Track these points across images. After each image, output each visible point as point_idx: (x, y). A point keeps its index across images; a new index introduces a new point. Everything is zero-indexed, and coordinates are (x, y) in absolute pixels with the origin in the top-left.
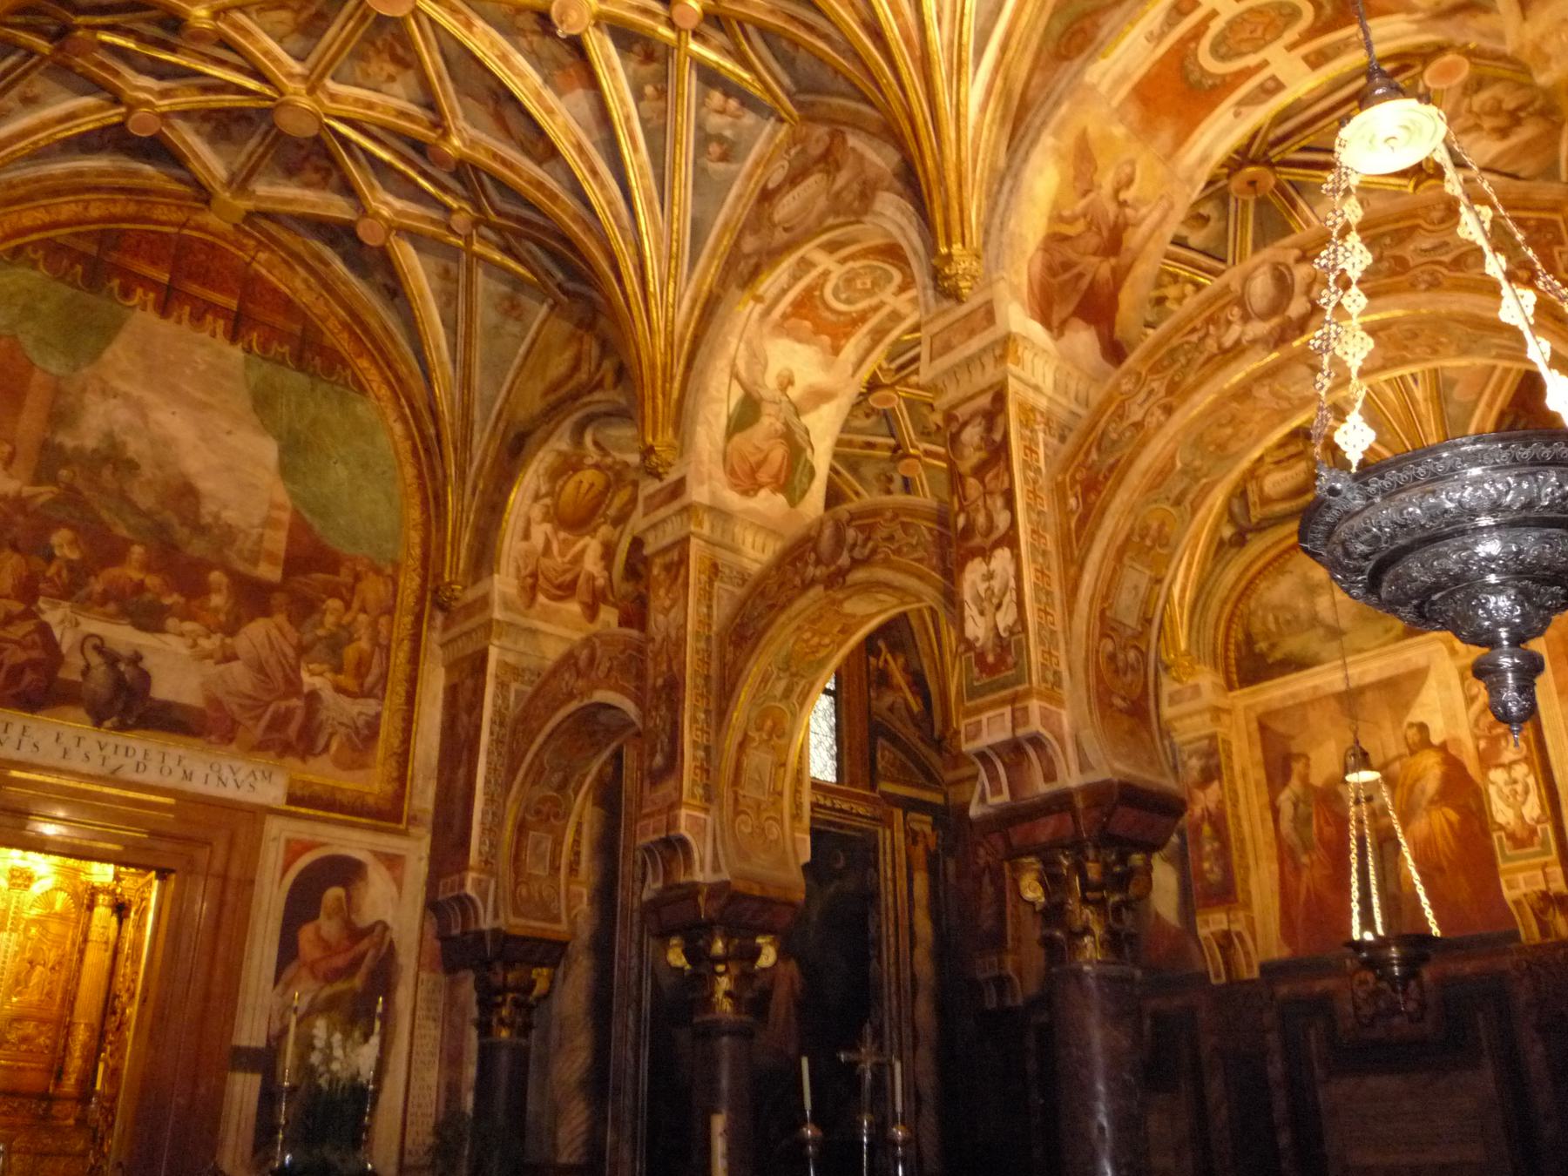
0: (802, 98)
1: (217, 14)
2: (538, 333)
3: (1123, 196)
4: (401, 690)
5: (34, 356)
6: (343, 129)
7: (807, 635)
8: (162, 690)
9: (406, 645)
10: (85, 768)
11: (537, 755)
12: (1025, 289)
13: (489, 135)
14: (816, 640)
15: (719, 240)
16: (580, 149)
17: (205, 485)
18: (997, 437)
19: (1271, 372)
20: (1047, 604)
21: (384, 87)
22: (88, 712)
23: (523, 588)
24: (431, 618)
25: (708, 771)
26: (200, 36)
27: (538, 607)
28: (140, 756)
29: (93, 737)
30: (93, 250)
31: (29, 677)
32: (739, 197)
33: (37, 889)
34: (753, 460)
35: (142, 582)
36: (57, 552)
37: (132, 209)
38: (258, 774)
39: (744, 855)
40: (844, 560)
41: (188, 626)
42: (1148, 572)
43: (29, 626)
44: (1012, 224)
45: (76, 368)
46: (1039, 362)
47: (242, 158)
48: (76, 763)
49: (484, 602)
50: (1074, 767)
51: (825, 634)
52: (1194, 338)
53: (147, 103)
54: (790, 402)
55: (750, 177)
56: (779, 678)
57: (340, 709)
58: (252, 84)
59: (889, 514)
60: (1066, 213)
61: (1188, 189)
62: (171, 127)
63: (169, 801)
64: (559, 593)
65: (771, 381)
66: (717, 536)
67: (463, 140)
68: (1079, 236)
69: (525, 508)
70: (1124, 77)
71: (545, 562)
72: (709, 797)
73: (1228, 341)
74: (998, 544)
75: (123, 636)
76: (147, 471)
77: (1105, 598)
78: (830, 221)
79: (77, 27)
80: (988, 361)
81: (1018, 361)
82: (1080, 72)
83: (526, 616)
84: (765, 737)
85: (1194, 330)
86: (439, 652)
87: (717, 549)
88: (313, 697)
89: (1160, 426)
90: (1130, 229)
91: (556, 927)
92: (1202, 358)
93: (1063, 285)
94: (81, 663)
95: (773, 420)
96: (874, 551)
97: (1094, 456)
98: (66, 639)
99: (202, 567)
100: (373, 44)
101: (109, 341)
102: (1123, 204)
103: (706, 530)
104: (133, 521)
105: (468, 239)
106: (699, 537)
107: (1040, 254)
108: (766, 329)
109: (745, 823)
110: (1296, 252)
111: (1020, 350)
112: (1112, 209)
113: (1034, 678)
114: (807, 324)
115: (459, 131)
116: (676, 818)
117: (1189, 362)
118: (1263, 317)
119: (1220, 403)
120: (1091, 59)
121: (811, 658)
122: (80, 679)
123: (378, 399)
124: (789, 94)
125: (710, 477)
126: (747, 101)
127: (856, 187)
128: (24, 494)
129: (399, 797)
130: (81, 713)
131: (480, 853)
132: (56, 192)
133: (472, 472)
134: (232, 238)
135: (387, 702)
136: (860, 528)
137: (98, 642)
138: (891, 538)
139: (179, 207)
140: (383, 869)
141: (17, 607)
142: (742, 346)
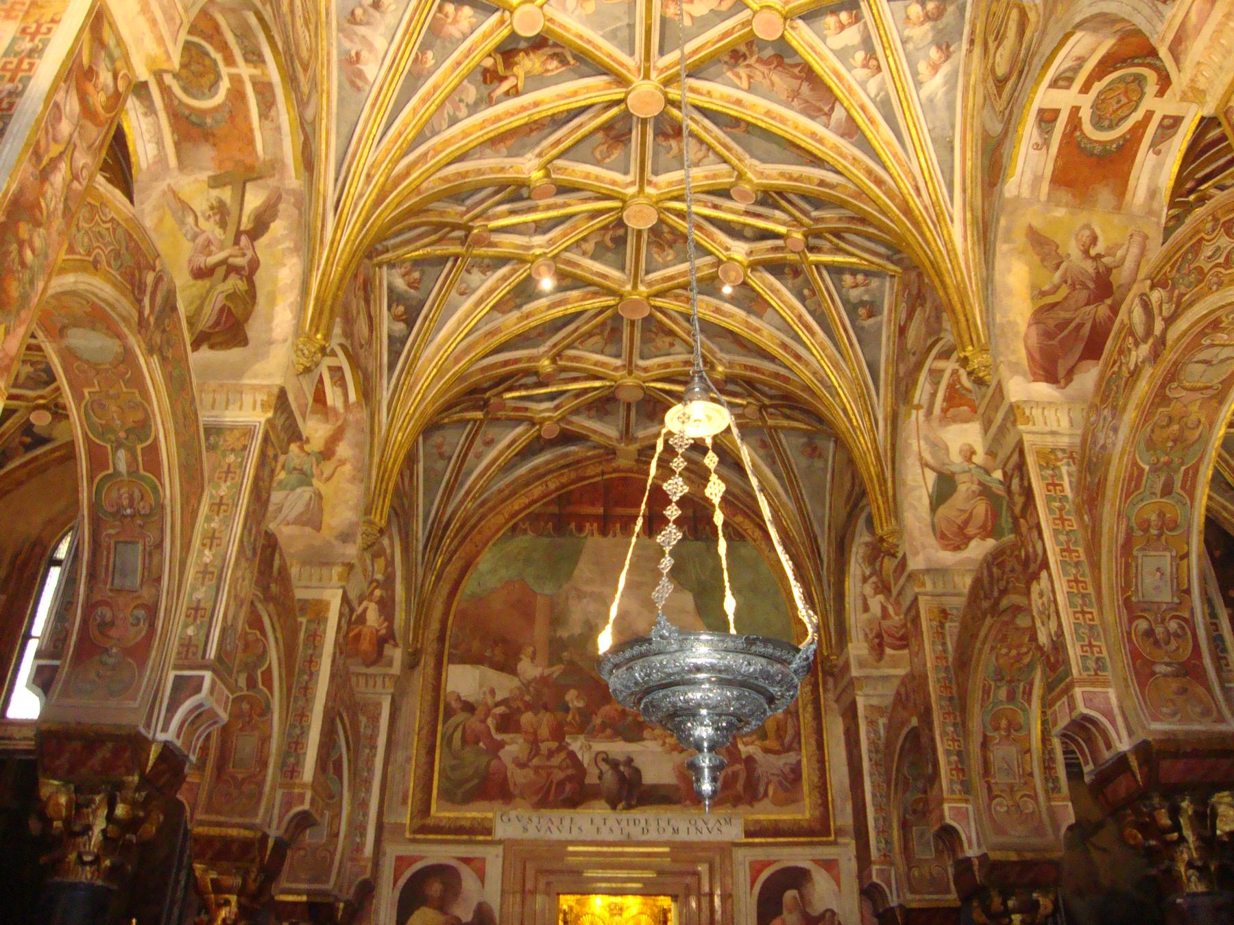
0: (896, 257)
1: (554, 361)
2: (834, 462)
3: (1093, 252)
4: (813, 742)
5: (536, 589)
6: (659, 385)
7: (1004, 651)
9: (810, 708)
10: (610, 838)
11: (898, 770)
12: (1024, 361)
13: (739, 354)
14: (1014, 652)
15: (886, 373)
16: (784, 346)
18: (1026, 484)
19: (1172, 376)
20: (1085, 604)
21: (672, 350)
23: (872, 648)
24: (825, 683)
25: (963, 770)
26: (548, 375)
27: (886, 658)
28: (643, 822)
30: (554, 509)
31: (568, 787)
32: (888, 338)
33: (626, 915)
34: (959, 521)
37: (573, 475)
38: (722, 821)
39: (1000, 830)
40: (996, 594)
42: (1168, 554)
43: (563, 755)
44: (998, 319)
45: (560, 587)
46: (1050, 413)
47: (621, 423)
48: (605, 835)
49: (846, 666)
50: (1124, 733)
51: (1019, 646)
52: (1116, 369)
53: (550, 418)
54: (978, 466)
55: (889, 321)
56: (998, 687)
57: (771, 764)
58: (597, 384)
59: (1008, 552)
60: (1046, 288)
61: (1154, 219)
62: (570, 423)
63: (666, 849)
64: (898, 643)
65: (956, 457)
66: (940, 589)
67: (723, 364)
68: (1066, 298)
69: (858, 590)
70: (1037, 180)
71: (886, 624)
72: (967, 788)
73: (1132, 367)
74: (1041, 569)
75: (618, 748)
77: (1127, 587)
78: (930, 342)
79: (489, 399)
80: (1009, 425)
81: (1028, 420)
82: (1001, 193)
83: (877, 668)
84: (1003, 733)
85: (1115, 362)
86: (835, 706)
87: (944, 599)
88: (750, 760)
89: (1114, 444)
90: (1114, 271)
91: (949, 897)
92: (1123, 383)
93: (1062, 342)
94: (597, 771)
95: (968, 485)
96: (1008, 582)
97: (1089, 479)
98: (586, 758)
100: (651, 331)
101: (576, 563)
102: (1099, 256)
103: (929, 587)
105: (762, 418)
106: (925, 594)
107: (1034, 329)
108: (935, 423)
109: (1001, 805)
110: (1148, 282)
111: (1027, 412)
112: (1089, 267)
113: (1075, 671)
114: (965, 408)
115: (720, 360)
116: (942, 811)
117: (1117, 387)
118: (1145, 341)
119: (1146, 414)
120: (1004, 182)
121: (1017, 665)
122: (597, 781)
123: (755, 540)
124: (888, 258)
125: (924, 547)
126: (867, 274)
127: (933, 314)
129: (825, 818)
130: (603, 803)
131: (879, 850)
132: (528, 484)
133: (824, 573)
134: (635, 469)
135: (804, 751)
136: (1001, 565)
138: (1012, 570)
139: (600, 462)
140: (823, 871)
141: (554, 745)
142: (922, 443)
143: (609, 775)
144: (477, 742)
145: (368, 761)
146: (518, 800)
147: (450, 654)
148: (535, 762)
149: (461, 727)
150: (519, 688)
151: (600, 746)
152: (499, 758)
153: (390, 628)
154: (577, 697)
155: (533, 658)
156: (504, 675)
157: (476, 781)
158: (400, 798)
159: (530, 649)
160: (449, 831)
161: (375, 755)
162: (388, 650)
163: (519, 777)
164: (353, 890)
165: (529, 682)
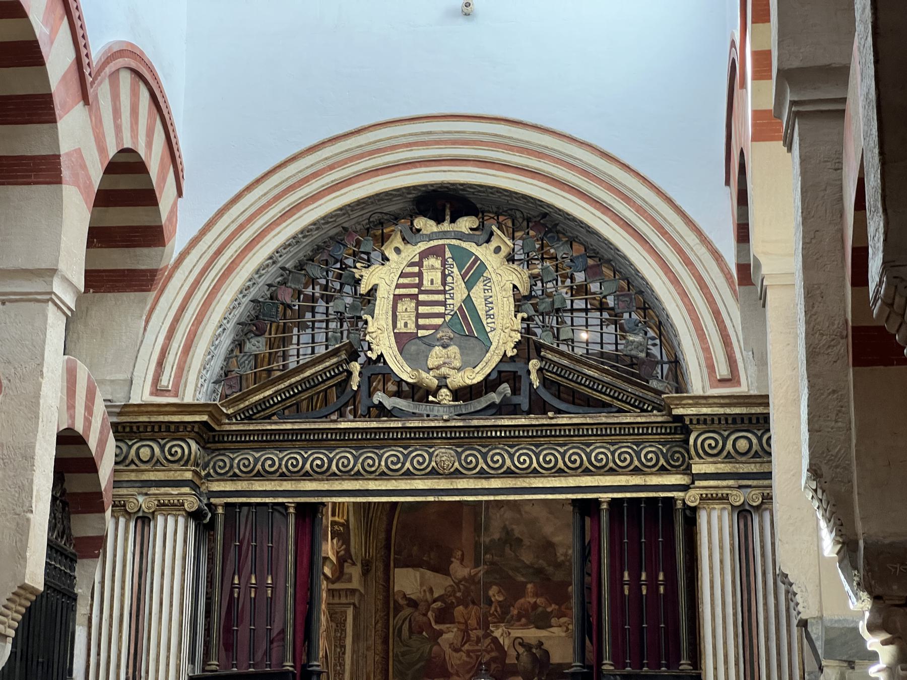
17: (557, 539)
35: (535, 602)
36: (493, 599)
43: (488, 641)
75: (532, 634)
76: (526, 542)
98: (506, 642)
128: (472, 574)
143: (525, 657)
144: (421, 633)
147: (395, 558)
148: (466, 647)
149: (407, 622)
150: (451, 586)
151: (516, 633)
152: (439, 645)
153: (348, 550)
154: (499, 592)
155: (462, 560)
159: (460, 553)
161: (344, 653)
162: (348, 569)
165: (460, 581)
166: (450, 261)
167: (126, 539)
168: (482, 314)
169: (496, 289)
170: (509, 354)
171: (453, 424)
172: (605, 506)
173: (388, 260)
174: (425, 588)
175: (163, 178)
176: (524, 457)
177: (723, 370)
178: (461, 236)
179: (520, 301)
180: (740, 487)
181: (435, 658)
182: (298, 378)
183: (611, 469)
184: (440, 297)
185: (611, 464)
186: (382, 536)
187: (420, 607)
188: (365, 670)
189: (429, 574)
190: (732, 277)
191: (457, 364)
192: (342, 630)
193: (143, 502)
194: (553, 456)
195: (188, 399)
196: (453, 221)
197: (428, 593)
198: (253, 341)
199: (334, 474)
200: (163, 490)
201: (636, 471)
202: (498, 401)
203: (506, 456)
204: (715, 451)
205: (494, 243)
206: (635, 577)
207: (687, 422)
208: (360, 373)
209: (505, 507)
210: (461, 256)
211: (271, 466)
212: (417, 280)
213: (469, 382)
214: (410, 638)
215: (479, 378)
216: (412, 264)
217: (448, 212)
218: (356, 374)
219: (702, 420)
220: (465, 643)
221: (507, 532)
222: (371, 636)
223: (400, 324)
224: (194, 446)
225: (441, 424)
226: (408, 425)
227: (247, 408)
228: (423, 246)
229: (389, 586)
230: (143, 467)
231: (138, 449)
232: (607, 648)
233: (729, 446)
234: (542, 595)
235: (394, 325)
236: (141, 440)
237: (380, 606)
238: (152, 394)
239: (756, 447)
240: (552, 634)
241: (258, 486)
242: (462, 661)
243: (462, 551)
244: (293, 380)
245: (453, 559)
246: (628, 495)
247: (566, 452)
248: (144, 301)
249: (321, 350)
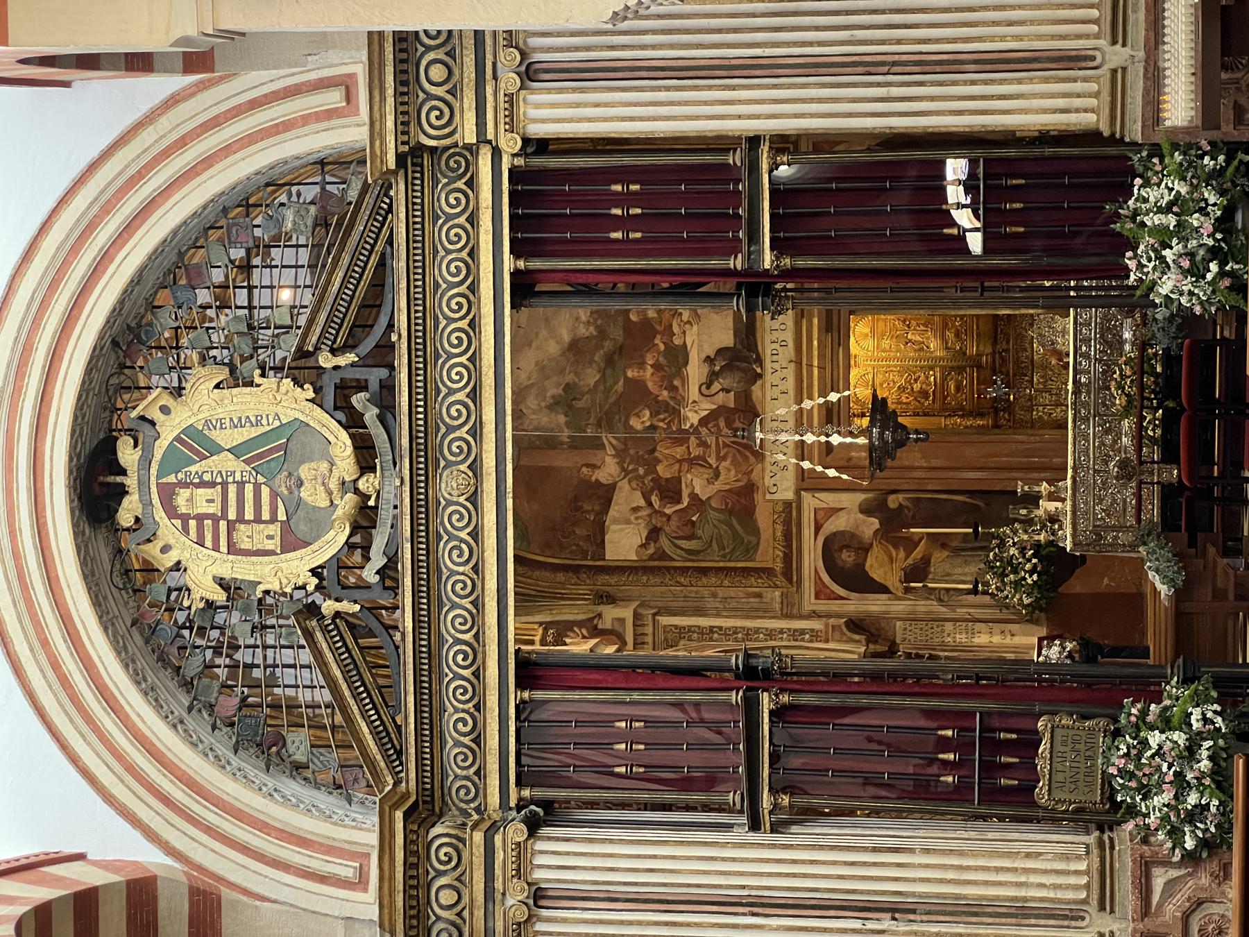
8: (728, 339)
17: (566, 337)
22: (753, 385)
28: (774, 346)
29: (769, 378)
35: (652, 366)
36: (648, 424)
41: (676, 329)
43: (704, 431)
75: (695, 371)
76: (570, 378)
98: (707, 407)
99: (628, 326)
104: (610, 382)
128: (614, 453)
137: (704, 386)
144: (693, 523)
145: (725, 634)
146: (755, 476)
147: (593, 559)
148: (712, 461)
149: (678, 542)
150: (630, 482)
151: (693, 392)
152: (709, 498)
153: (580, 624)
154: (638, 415)
155: (594, 467)
156: (615, 497)
157: (734, 522)
158: (757, 600)
159: (584, 470)
160: (788, 546)
161: (720, 628)
162: (606, 623)
163: (729, 477)
164: (857, 637)
165: (623, 469)
166: (180, 476)
167: (564, 921)
168: (255, 432)
169: (220, 412)
170: (311, 394)
171: (406, 473)
172: (521, 264)
173: (179, 563)
174: (632, 518)
175: (58, 881)
176: (452, 374)
177: (334, 98)
178: (146, 461)
179: (237, 379)
180: (495, 78)
181: (727, 504)
182: (344, 687)
183: (471, 254)
184: (232, 489)
185: (464, 254)
186: (561, 577)
187: (659, 525)
188: (743, 600)
189: (613, 512)
190: (201, 82)
191: (325, 466)
192: (689, 631)
193: (514, 899)
194: (450, 333)
195: (373, 839)
196: (123, 472)
197: (640, 514)
198: (292, 749)
199: (476, 636)
200: (498, 871)
201: (473, 219)
202: (376, 411)
203: (452, 399)
204: (446, 111)
205: (155, 414)
206: (618, 223)
207: (406, 148)
208: (338, 600)
209: (522, 407)
210: (173, 461)
211: (465, 725)
212: (208, 522)
213: (350, 450)
214: (700, 538)
215: (344, 436)
216: (186, 530)
217: (111, 479)
218: (338, 606)
219: (403, 127)
220: (707, 462)
221: (555, 405)
222: (696, 592)
223: (269, 545)
224: (438, 830)
225: (407, 488)
226: (408, 534)
227: (386, 757)
228: (160, 514)
229: (629, 567)
230: (466, 899)
231: (441, 907)
232: (714, 263)
233: (439, 92)
234: (642, 357)
235: (272, 553)
236: (429, 902)
237: (658, 580)
238: (365, 890)
239: (440, 54)
240: (695, 345)
241: (493, 741)
242: (732, 467)
243: (582, 466)
244: (347, 693)
245: (593, 479)
246: (506, 231)
247: (446, 317)
248: (234, 903)
249: (306, 656)
